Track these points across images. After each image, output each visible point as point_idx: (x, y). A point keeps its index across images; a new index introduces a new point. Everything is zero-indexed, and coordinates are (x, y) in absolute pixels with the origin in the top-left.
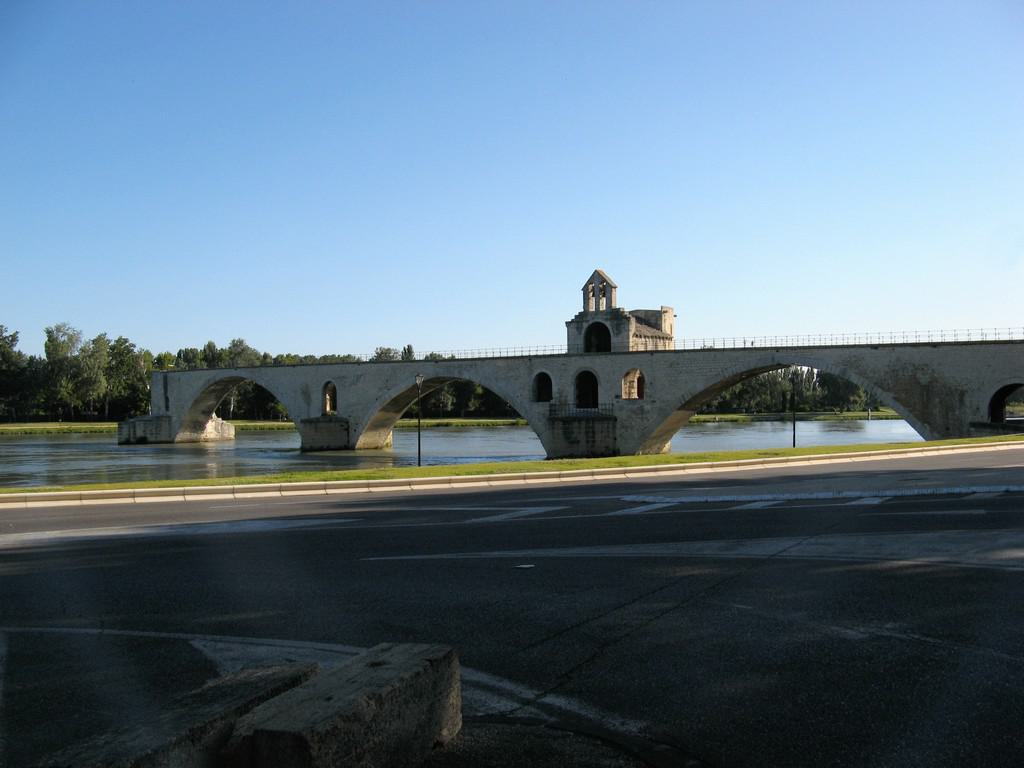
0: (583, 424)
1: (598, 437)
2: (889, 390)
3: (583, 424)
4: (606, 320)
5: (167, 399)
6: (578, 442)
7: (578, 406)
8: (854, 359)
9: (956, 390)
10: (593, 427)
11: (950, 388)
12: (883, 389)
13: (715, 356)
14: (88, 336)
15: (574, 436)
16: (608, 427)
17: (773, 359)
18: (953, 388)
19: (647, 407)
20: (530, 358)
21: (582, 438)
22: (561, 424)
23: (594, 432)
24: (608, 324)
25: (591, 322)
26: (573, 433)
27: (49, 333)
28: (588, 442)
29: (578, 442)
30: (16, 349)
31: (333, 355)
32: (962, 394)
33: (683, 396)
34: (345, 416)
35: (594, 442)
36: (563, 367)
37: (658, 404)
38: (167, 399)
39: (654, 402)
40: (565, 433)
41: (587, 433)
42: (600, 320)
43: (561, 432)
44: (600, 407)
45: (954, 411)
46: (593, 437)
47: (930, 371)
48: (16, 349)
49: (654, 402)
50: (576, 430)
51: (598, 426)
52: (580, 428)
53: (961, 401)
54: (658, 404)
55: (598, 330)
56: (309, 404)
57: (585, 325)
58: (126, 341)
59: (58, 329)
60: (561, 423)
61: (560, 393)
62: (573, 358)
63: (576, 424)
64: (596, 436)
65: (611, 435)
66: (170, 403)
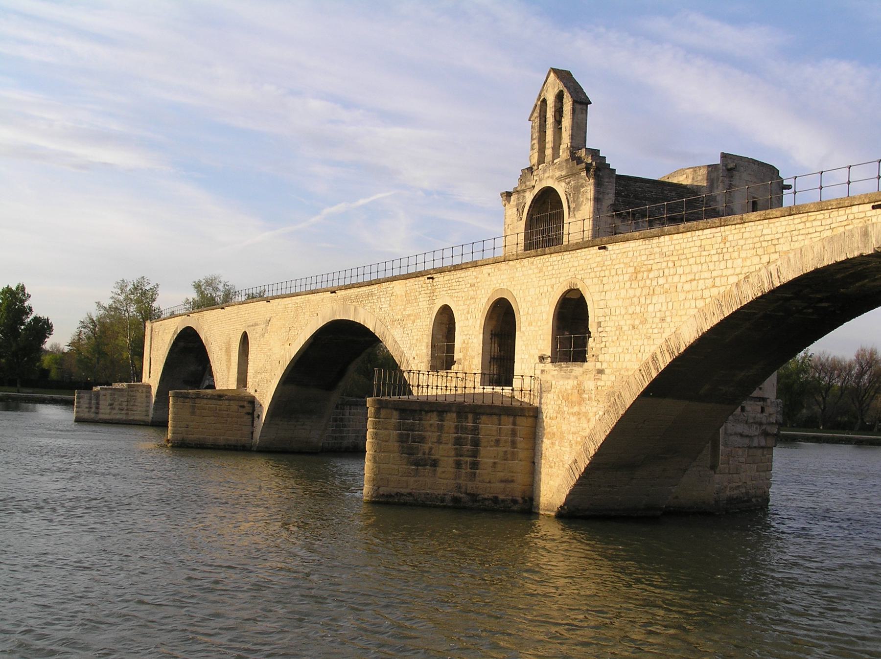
1: (487, 455)
4: (559, 179)
6: (435, 464)
7: (483, 383)
10: (476, 430)
13: (724, 240)
15: (426, 447)
16: (514, 433)
17: (865, 234)
19: (590, 385)
20: (429, 274)
21: (445, 453)
23: (476, 443)
24: (561, 189)
25: (536, 190)
26: (422, 439)
27: (198, 286)
28: (458, 465)
29: (435, 464)
33: (654, 358)
35: (475, 465)
37: (607, 380)
39: (601, 372)
40: (402, 439)
41: (458, 442)
42: (549, 183)
44: (517, 383)
46: (475, 454)
48: (155, 305)
49: (601, 372)
50: (431, 436)
52: (440, 428)
54: (607, 380)
57: (529, 197)
59: (210, 283)
60: (396, 414)
62: (486, 269)
63: (433, 419)
64: (483, 451)
65: (522, 454)
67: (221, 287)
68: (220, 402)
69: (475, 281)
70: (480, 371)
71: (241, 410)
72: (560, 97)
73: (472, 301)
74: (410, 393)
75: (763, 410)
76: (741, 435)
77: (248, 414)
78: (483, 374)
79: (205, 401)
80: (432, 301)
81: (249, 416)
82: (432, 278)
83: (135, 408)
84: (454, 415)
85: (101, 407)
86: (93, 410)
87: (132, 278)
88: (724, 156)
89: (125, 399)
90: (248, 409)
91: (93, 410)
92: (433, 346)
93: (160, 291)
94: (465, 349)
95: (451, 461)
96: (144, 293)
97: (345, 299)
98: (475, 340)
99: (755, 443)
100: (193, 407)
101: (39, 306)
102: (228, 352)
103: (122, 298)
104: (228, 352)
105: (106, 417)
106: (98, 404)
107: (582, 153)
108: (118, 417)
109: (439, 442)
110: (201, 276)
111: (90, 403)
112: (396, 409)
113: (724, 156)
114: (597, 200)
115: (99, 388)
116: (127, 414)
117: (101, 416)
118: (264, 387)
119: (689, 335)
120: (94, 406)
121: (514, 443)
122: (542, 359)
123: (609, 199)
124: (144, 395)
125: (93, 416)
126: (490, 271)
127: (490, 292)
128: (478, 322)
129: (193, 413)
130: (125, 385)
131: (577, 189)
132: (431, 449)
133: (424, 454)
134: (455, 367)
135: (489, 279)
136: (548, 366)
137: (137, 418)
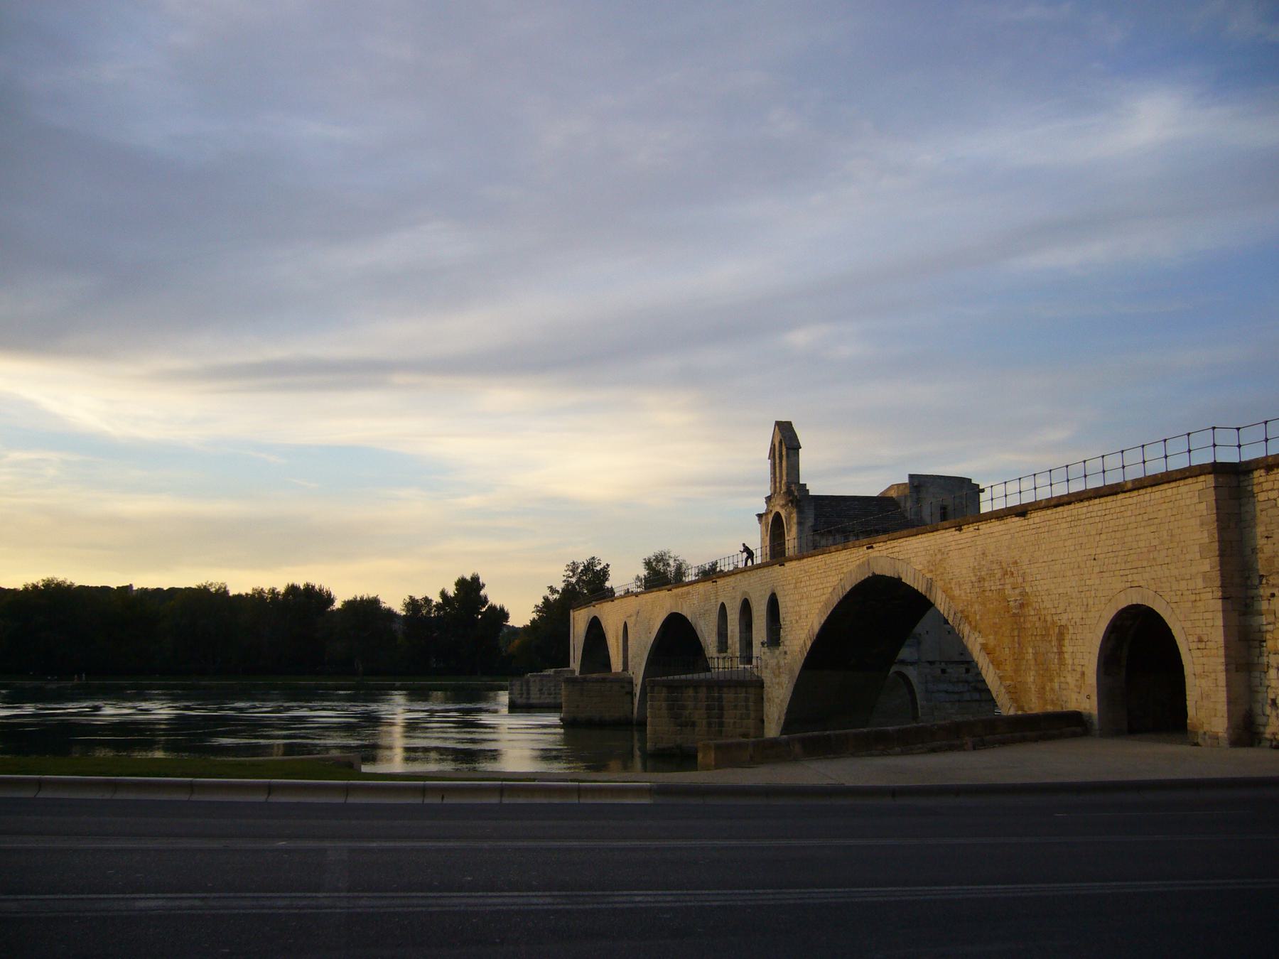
0: (703, 693)
2: (975, 628)
3: (703, 693)
4: (782, 506)
6: (694, 724)
8: (939, 557)
9: (1053, 623)
10: (720, 699)
11: (1045, 621)
12: (970, 623)
16: (747, 700)
18: (1049, 618)
19: (782, 663)
23: (721, 708)
27: (648, 564)
28: (709, 724)
29: (694, 724)
30: (608, 584)
31: (159, 589)
32: (1061, 637)
35: (721, 724)
41: (709, 708)
42: (778, 509)
43: (664, 704)
44: (754, 661)
45: (1051, 680)
46: (721, 716)
47: (1020, 580)
48: (608, 584)
51: (728, 696)
53: (1061, 653)
55: (960, 530)
59: (661, 558)
60: (665, 690)
63: (691, 692)
65: (752, 715)
67: (671, 562)
72: (781, 443)
74: (708, 669)
75: (967, 671)
76: (947, 692)
84: (704, 689)
87: (582, 559)
88: (911, 476)
93: (611, 571)
95: (705, 722)
96: (597, 574)
97: (677, 595)
99: (967, 696)
101: (494, 595)
103: (574, 580)
107: (793, 488)
110: (650, 553)
113: (911, 476)
114: (800, 524)
118: (638, 671)
119: (817, 629)
121: (747, 708)
122: (763, 644)
123: (810, 522)
131: (790, 513)
136: (766, 649)
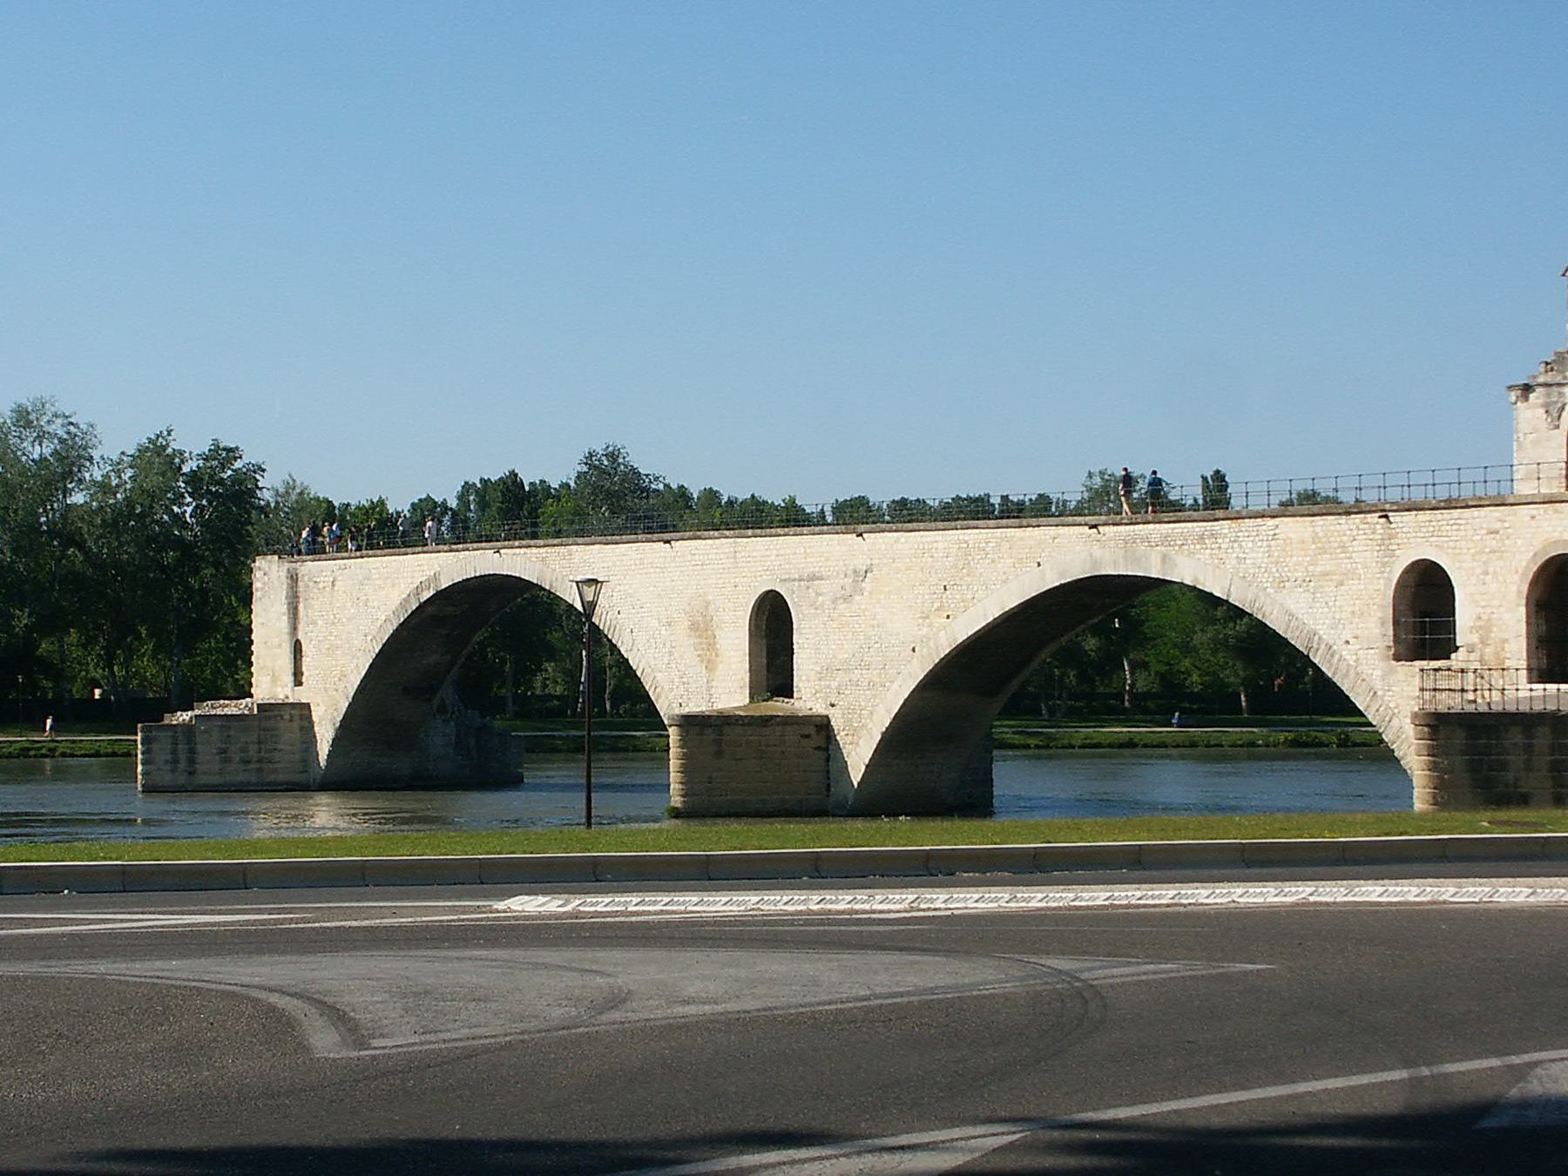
5: (297, 649)
14: (115, 443)
15: (1510, 776)
22: (1459, 738)
26: (1503, 766)
34: (819, 709)
36: (1491, 543)
38: (297, 649)
50: (1516, 759)
52: (1529, 749)
56: (710, 667)
58: (232, 453)
61: (1484, 628)
66: (306, 661)
68: (768, 731)
69: (1498, 525)
70: (1524, 664)
71: (805, 742)
73: (1494, 557)
77: (818, 748)
78: (1529, 669)
79: (739, 730)
80: (1386, 548)
81: (821, 753)
82: (1386, 517)
83: (277, 755)
85: (200, 758)
86: (182, 765)
89: (255, 738)
90: (818, 740)
91: (182, 765)
92: (1396, 623)
94: (1484, 628)
98: (1507, 616)
100: (718, 743)
102: (703, 629)
104: (703, 629)
105: (215, 780)
106: (192, 751)
108: (239, 778)
109: (1528, 768)
111: (174, 752)
112: (1461, 726)
115: (184, 717)
116: (259, 770)
117: (202, 779)
120: (183, 757)
124: (296, 724)
125: (182, 779)
126: (1534, 512)
127: (1538, 545)
128: (1514, 588)
129: (719, 753)
130: (232, 708)
132: (1517, 779)
133: (1507, 786)
134: (1457, 660)
135: (1533, 523)
137: (281, 777)
